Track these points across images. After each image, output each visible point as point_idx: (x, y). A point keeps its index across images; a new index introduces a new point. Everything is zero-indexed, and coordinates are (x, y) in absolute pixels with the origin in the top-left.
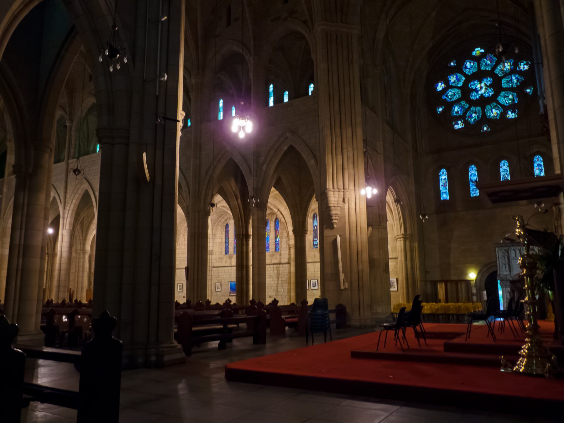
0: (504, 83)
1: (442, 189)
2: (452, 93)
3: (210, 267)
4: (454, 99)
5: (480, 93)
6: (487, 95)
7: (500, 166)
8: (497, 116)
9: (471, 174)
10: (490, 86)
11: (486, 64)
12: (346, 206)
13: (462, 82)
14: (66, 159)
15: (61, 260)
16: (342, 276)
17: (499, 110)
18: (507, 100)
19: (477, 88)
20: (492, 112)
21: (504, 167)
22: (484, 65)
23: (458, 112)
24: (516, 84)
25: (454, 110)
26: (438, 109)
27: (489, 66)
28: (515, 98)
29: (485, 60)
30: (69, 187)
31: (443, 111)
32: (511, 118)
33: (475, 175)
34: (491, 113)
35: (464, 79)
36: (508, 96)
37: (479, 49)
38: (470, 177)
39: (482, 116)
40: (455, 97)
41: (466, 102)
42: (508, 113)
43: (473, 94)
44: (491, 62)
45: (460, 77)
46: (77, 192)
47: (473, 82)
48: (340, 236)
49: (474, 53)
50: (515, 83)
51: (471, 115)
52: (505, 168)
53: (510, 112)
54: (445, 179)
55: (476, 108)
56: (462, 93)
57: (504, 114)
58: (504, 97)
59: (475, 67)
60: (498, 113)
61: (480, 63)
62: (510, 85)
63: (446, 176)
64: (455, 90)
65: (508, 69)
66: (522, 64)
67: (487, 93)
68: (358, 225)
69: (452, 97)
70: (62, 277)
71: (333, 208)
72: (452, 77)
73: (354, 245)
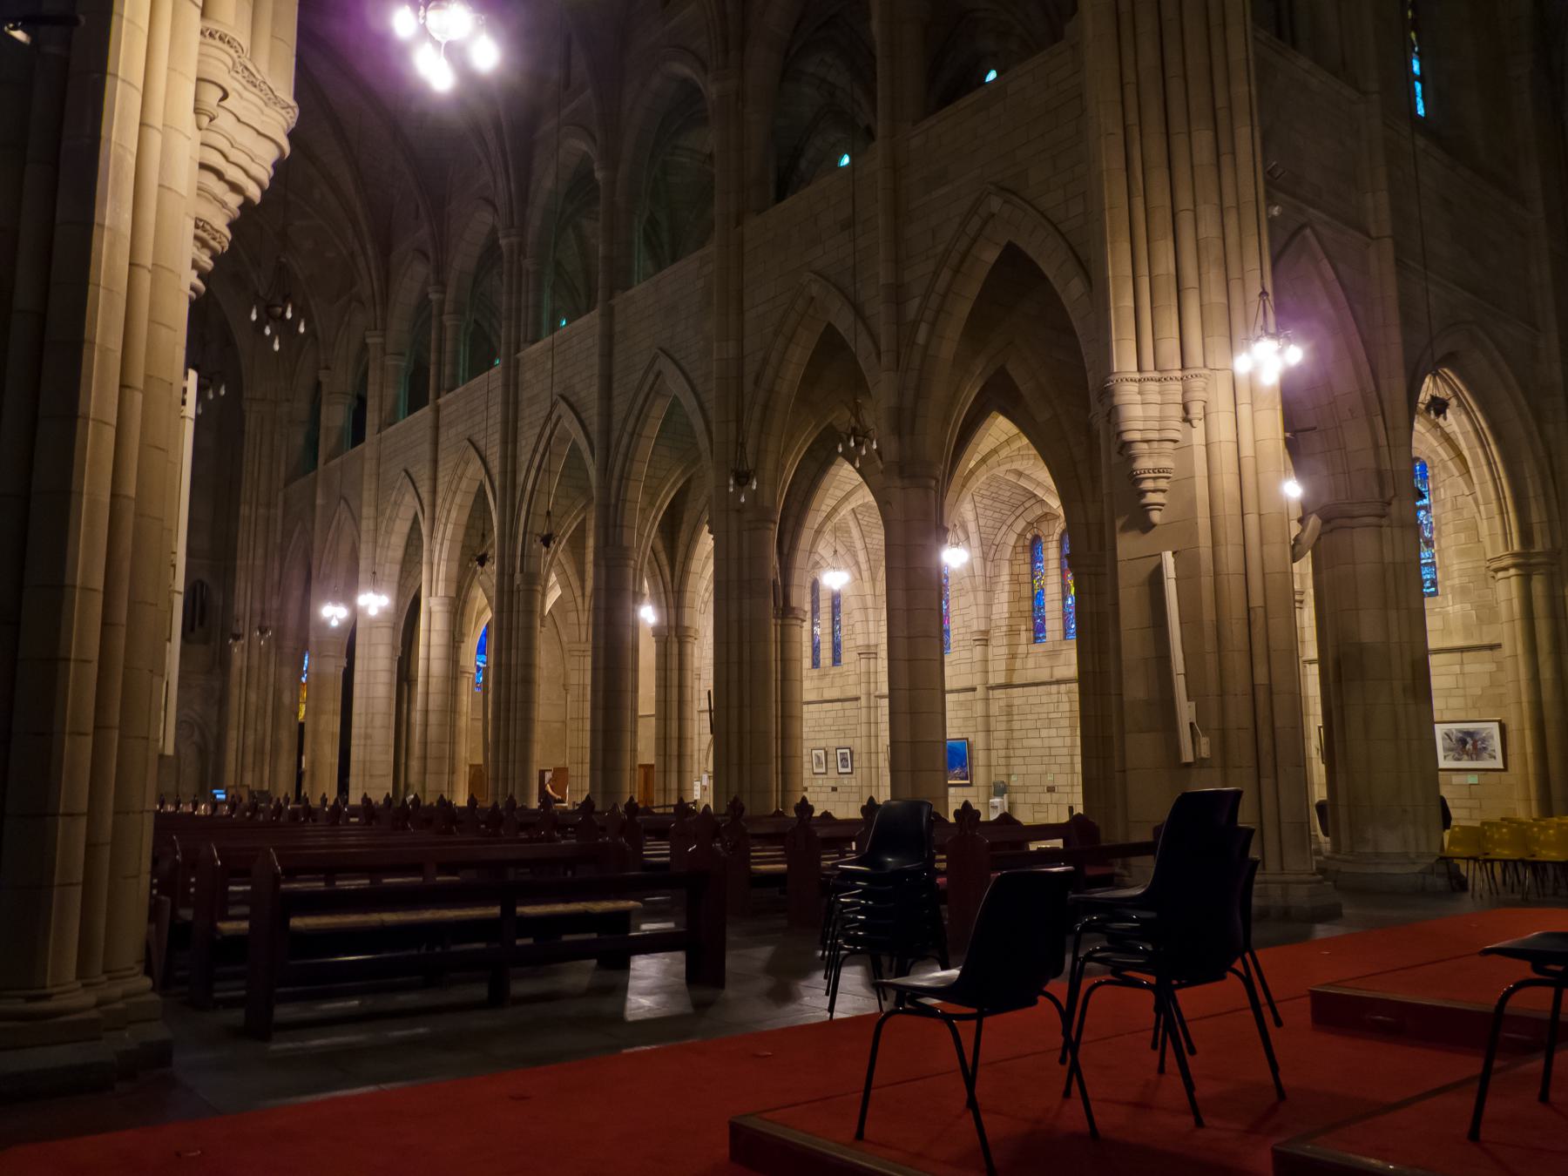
3: (872, 697)
12: (1198, 435)
14: (431, 395)
15: (427, 683)
16: (1186, 711)
30: (440, 475)
46: (457, 488)
48: (1174, 553)
68: (1250, 506)
70: (433, 732)
71: (1145, 446)
73: (1233, 587)
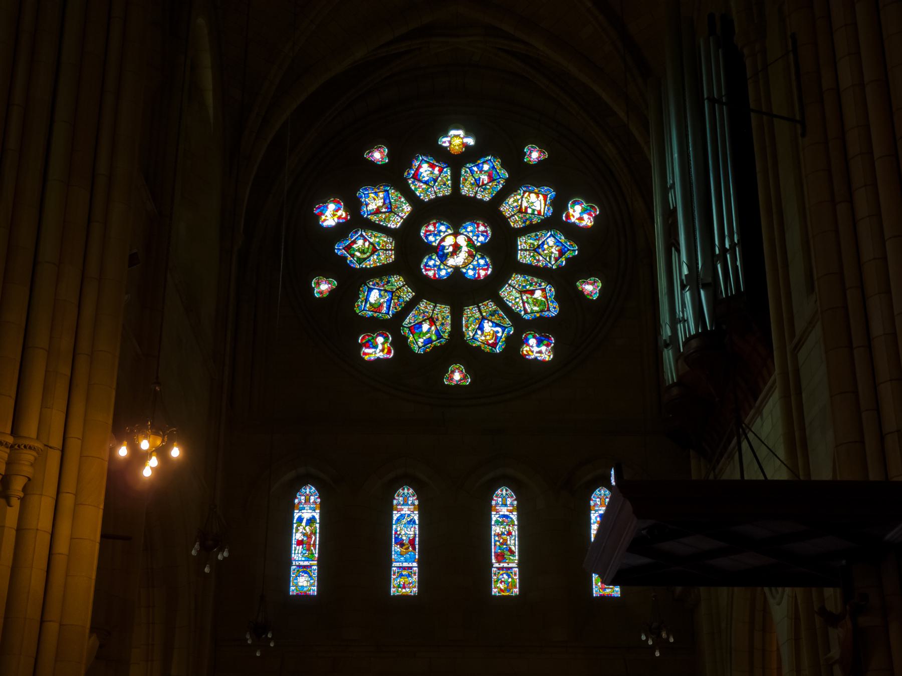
0: (522, 250)
1: (298, 555)
2: (367, 244)
4: (367, 264)
5: (451, 262)
6: (471, 273)
7: (491, 506)
8: (494, 345)
9: (398, 515)
10: (483, 250)
11: (477, 183)
13: (402, 218)
17: (504, 329)
18: (528, 303)
19: (444, 247)
20: (481, 328)
21: (504, 511)
22: (472, 184)
23: (377, 308)
24: (556, 259)
25: (367, 300)
26: (318, 284)
27: (485, 189)
28: (552, 302)
29: (475, 169)
31: (332, 292)
32: (536, 358)
33: (412, 522)
34: (479, 332)
35: (407, 208)
36: (532, 292)
37: (461, 133)
38: (394, 527)
39: (451, 334)
40: (375, 257)
41: (408, 283)
42: (526, 342)
43: (431, 263)
44: (491, 179)
45: (395, 201)
47: (434, 225)
49: (444, 141)
50: (553, 255)
51: (420, 324)
52: (508, 513)
53: (532, 341)
54: (311, 521)
55: (435, 307)
56: (398, 250)
57: (515, 342)
58: (522, 292)
59: (445, 184)
60: (499, 335)
61: (460, 175)
62: (538, 261)
63: (318, 511)
64: (375, 236)
65: (536, 213)
66: (578, 208)
67: (471, 267)
69: (365, 256)
72: (372, 195)
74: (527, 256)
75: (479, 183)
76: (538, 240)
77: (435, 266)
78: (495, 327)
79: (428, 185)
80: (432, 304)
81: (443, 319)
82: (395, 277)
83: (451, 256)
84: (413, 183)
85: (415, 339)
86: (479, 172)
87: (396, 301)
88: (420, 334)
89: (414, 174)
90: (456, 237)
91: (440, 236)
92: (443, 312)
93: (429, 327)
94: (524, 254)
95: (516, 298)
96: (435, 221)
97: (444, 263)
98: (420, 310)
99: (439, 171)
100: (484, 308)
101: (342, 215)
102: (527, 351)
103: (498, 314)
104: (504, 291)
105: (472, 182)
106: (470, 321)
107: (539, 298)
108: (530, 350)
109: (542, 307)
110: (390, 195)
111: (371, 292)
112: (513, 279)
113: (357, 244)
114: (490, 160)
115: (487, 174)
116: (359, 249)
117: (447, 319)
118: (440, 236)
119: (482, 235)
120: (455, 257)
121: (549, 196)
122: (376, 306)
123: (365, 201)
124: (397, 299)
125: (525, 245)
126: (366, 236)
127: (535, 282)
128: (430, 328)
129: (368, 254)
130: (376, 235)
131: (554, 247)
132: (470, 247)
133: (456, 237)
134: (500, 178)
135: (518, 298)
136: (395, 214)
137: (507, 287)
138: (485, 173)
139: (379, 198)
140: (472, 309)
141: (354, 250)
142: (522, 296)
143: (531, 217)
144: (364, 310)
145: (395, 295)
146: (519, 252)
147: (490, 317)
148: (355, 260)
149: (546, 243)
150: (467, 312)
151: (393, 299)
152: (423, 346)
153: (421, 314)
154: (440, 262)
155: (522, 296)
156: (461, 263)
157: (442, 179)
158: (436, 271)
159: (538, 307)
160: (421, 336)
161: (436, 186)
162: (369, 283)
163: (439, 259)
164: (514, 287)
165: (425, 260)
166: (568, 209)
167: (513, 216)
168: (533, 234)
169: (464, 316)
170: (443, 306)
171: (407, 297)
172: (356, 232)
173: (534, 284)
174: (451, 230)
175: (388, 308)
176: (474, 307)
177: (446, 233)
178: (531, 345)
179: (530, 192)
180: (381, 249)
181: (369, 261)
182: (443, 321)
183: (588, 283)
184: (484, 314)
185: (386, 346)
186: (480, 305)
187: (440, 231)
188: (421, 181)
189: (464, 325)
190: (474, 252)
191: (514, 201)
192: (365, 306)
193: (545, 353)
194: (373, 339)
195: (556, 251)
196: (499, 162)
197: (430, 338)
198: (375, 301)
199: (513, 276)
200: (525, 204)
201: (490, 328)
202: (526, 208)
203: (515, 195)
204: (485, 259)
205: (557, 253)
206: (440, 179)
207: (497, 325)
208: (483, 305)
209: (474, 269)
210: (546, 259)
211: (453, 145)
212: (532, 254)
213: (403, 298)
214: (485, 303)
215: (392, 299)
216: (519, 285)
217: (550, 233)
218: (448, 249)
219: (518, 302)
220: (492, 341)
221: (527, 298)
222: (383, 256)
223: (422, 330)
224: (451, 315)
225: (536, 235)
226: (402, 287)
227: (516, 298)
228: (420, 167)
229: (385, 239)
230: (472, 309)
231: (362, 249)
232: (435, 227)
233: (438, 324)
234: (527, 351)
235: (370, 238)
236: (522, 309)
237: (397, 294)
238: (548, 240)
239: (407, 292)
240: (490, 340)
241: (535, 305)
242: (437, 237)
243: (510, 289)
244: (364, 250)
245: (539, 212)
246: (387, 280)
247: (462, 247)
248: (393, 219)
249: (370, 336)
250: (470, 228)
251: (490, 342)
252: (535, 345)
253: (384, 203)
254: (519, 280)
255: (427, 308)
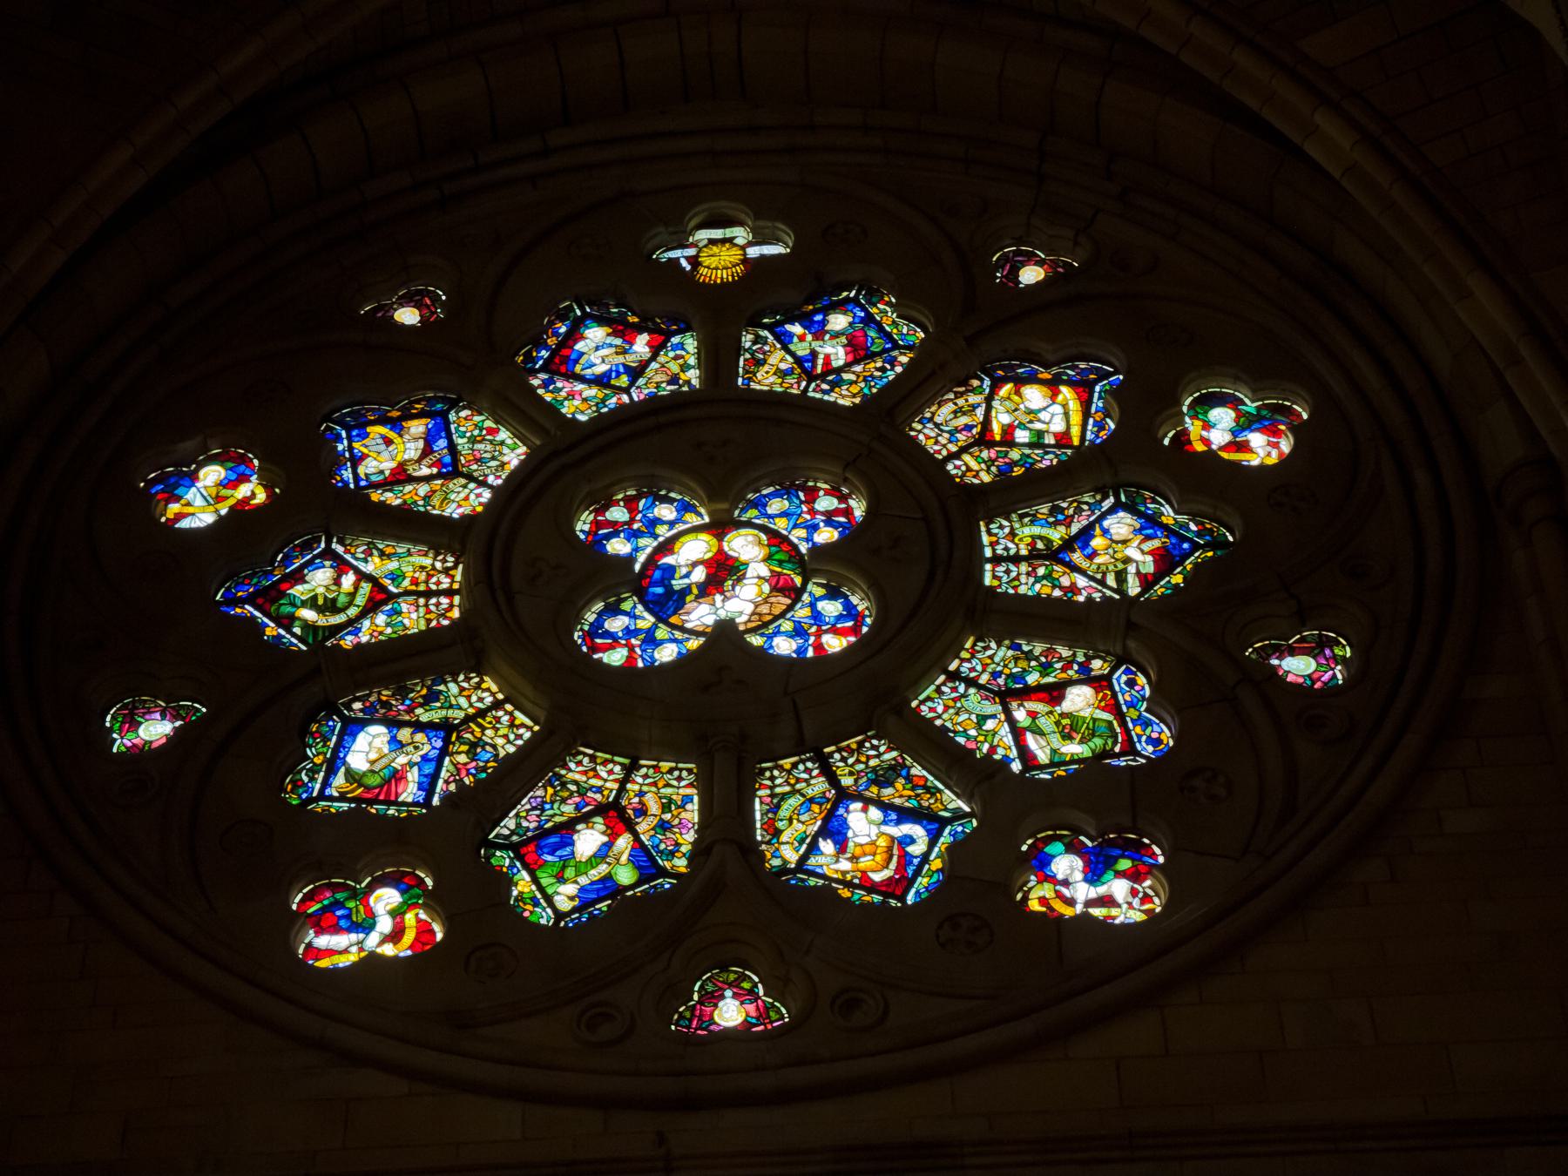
0: (997, 560)
2: (348, 580)
18: (1039, 732)
19: (671, 570)
20: (834, 829)
27: (835, 385)
28: (1146, 724)
34: (827, 846)
36: (1054, 694)
42: (1041, 862)
43: (616, 624)
45: (473, 440)
47: (631, 504)
50: (1132, 569)
55: (629, 770)
62: (1073, 589)
64: (382, 554)
65: (1049, 440)
67: (787, 626)
69: (339, 619)
74: (1023, 579)
75: (814, 366)
76: (1068, 522)
77: (630, 632)
78: (899, 822)
79: (608, 386)
80: (617, 759)
81: (666, 808)
82: (461, 677)
83: (698, 597)
84: (545, 385)
85: (541, 889)
86: (809, 337)
87: (462, 759)
88: (564, 867)
89: (548, 361)
90: (720, 537)
91: (656, 537)
92: (668, 785)
93: (606, 839)
94: (1008, 572)
95: (983, 719)
96: (631, 492)
97: (673, 620)
98: (564, 785)
99: (649, 344)
100: (844, 759)
101: (253, 495)
102: (1043, 901)
103: (909, 778)
104: (929, 699)
105: (783, 366)
106: (784, 812)
107: (1086, 713)
108: (1059, 895)
109: (1098, 742)
110: (453, 427)
111: (354, 735)
112: (964, 655)
113: (306, 582)
114: (856, 298)
115: (844, 340)
116: (315, 598)
117: (682, 807)
118: (656, 537)
119: (829, 522)
120: (718, 598)
121: (1097, 388)
122: (374, 781)
123: (351, 449)
124: (467, 753)
125: (1010, 545)
126: (348, 557)
127: (1061, 659)
128: (608, 845)
129: (353, 612)
130: (389, 550)
131: (1135, 543)
132: (780, 563)
133: (720, 537)
134: (896, 346)
135: (993, 716)
136: (470, 477)
137: (944, 684)
138: (832, 338)
139: (407, 437)
140: (795, 766)
141: (293, 605)
142: (1008, 712)
143: (1028, 456)
144: (322, 796)
145: (458, 738)
146: (988, 567)
147: (874, 789)
148: (294, 635)
149: (1098, 531)
150: (772, 778)
151: (452, 754)
152: (574, 910)
153: (571, 796)
154: (653, 620)
155: (1008, 712)
156: (744, 618)
157: (663, 366)
158: (638, 650)
159: (1082, 742)
160: (569, 873)
161: (638, 387)
162: (348, 706)
163: (647, 609)
164: (971, 683)
165: (591, 617)
166: (1183, 422)
167: (956, 456)
168: (1044, 509)
169: (760, 793)
170: (665, 766)
171: (509, 742)
172: (307, 546)
173: (1058, 666)
174: (700, 515)
175: (428, 786)
176: (803, 761)
177: (680, 527)
178: (1060, 877)
179: (1020, 382)
180: (407, 593)
181: (356, 632)
182: (667, 816)
183: (1293, 652)
184: (847, 781)
185: (410, 918)
186: (827, 750)
187: (657, 521)
188: (582, 379)
189: (758, 825)
190: (798, 581)
191: (955, 412)
192: (326, 784)
193: (1130, 904)
194: (354, 894)
195: (1143, 552)
196: (889, 304)
197: (608, 878)
198: (373, 762)
199: (968, 645)
200: (1001, 418)
201: (874, 830)
202: (1009, 430)
203: (958, 395)
204: (846, 597)
205: (1149, 558)
206: (654, 365)
207: (905, 815)
208: (839, 750)
209: (799, 631)
210: (1102, 582)
211: (708, 267)
212: (1041, 571)
213: (494, 746)
214: (852, 742)
215: (444, 752)
216: (995, 675)
217: (1112, 499)
218: (687, 575)
219: (995, 733)
220: (887, 874)
221: (1033, 715)
222: (414, 616)
223: (573, 853)
224: (698, 794)
225: (1055, 510)
226: (489, 709)
227: (983, 719)
228: (574, 335)
229: (427, 561)
230: (795, 766)
231: (326, 597)
232: (633, 510)
233: (643, 826)
234: (1043, 901)
235: (366, 561)
236: (1014, 753)
237: (468, 736)
238: (1106, 524)
239: (512, 725)
240: (873, 871)
241: (1068, 737)
242: (642, 542)
243: (954, 689)
244: (334, 600)
245: (1063, 439)
246: (424, 691)
247: (746, 564)
248: (462, 495)
249: (344, 887)
250: (776, 506)
251: (877, 877)
252: (1078, 876)
253: (427, 451)
254: (991, 657)
255: (597, 776)
